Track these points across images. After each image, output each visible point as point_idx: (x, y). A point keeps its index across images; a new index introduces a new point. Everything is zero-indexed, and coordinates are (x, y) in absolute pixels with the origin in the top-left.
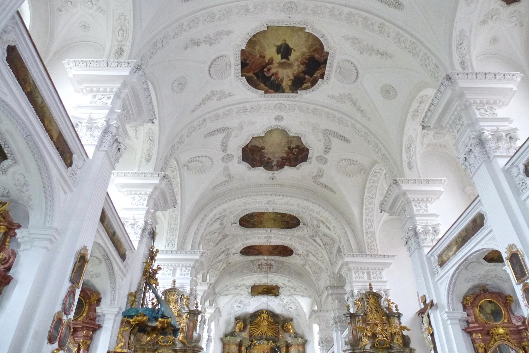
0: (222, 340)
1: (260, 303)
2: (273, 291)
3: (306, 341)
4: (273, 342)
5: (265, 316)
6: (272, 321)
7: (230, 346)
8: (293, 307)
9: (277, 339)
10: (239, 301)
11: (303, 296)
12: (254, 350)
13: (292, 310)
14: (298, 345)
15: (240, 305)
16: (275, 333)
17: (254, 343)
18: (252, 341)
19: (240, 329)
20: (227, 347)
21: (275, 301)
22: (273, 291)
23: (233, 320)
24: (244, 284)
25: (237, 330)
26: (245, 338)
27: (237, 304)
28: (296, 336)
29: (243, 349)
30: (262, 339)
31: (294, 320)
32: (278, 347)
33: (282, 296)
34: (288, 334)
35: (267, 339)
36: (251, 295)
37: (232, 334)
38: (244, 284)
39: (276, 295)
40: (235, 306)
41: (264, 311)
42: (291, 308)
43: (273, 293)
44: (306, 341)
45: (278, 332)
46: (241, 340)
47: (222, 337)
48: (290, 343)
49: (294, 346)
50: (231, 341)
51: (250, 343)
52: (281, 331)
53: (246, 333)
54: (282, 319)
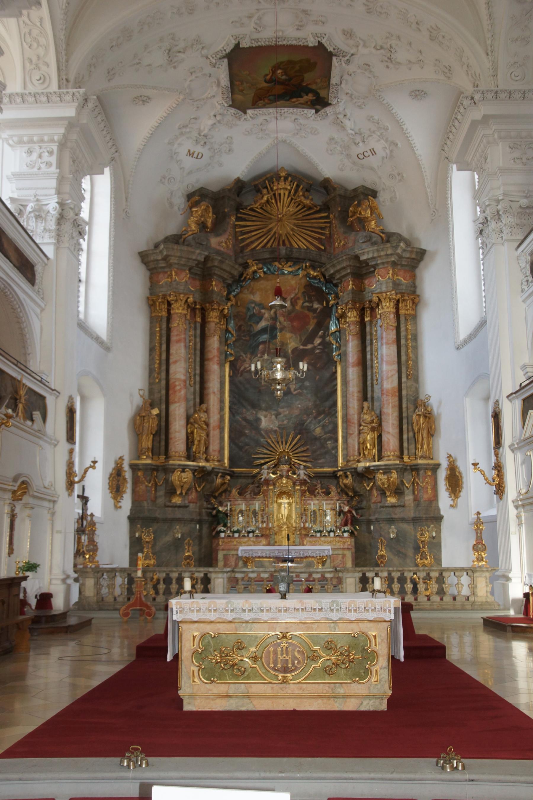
0: (144, 257)
1: (267, 143)
2: (308, 77)
3: (422, 254)
4: (314, 268)
5: (282, 188)
6: (307, 202)
7: (171, 276)
8: (379, 146)
9: (324, 259)
10: (195, 134)
11: (418, 94)
12: (252, 293)
13: (373, 161)
14: (394, 264)
15: (198, 149)
16: (320, 240)
17: (251, 270)
18: (246, 266)
19: (202, 226)
20: (163, 280)
21: (314, 132)
22: (308, 77)
23: (180, 201)
24: (198, 41)
25: (193, 227)
26: (218, 253)
27: (188, 145)
28: (388, 238)
29: (216, 286)
30: (278, 259)
31: (383, 197)
32: (329, 281)
33: (341, 103)
34: (362, 234)
35: (293, 259)
36: (234, 105)
37: (176, 239)
38: (198, 41)
39: (320, 103)
40: (183, 151)
41: (283, 174)
42: (373, 152)
43: (308, 91)
44: (422, 254)
45: (330, 237)
46: (207, 258)
47: (143, 248)
48: (366, 262)
49: (380, 270)
50: (173, 260)
51: (240, 269)
52: (339, 231)
53: (223, 239)
54: (342, 192)
